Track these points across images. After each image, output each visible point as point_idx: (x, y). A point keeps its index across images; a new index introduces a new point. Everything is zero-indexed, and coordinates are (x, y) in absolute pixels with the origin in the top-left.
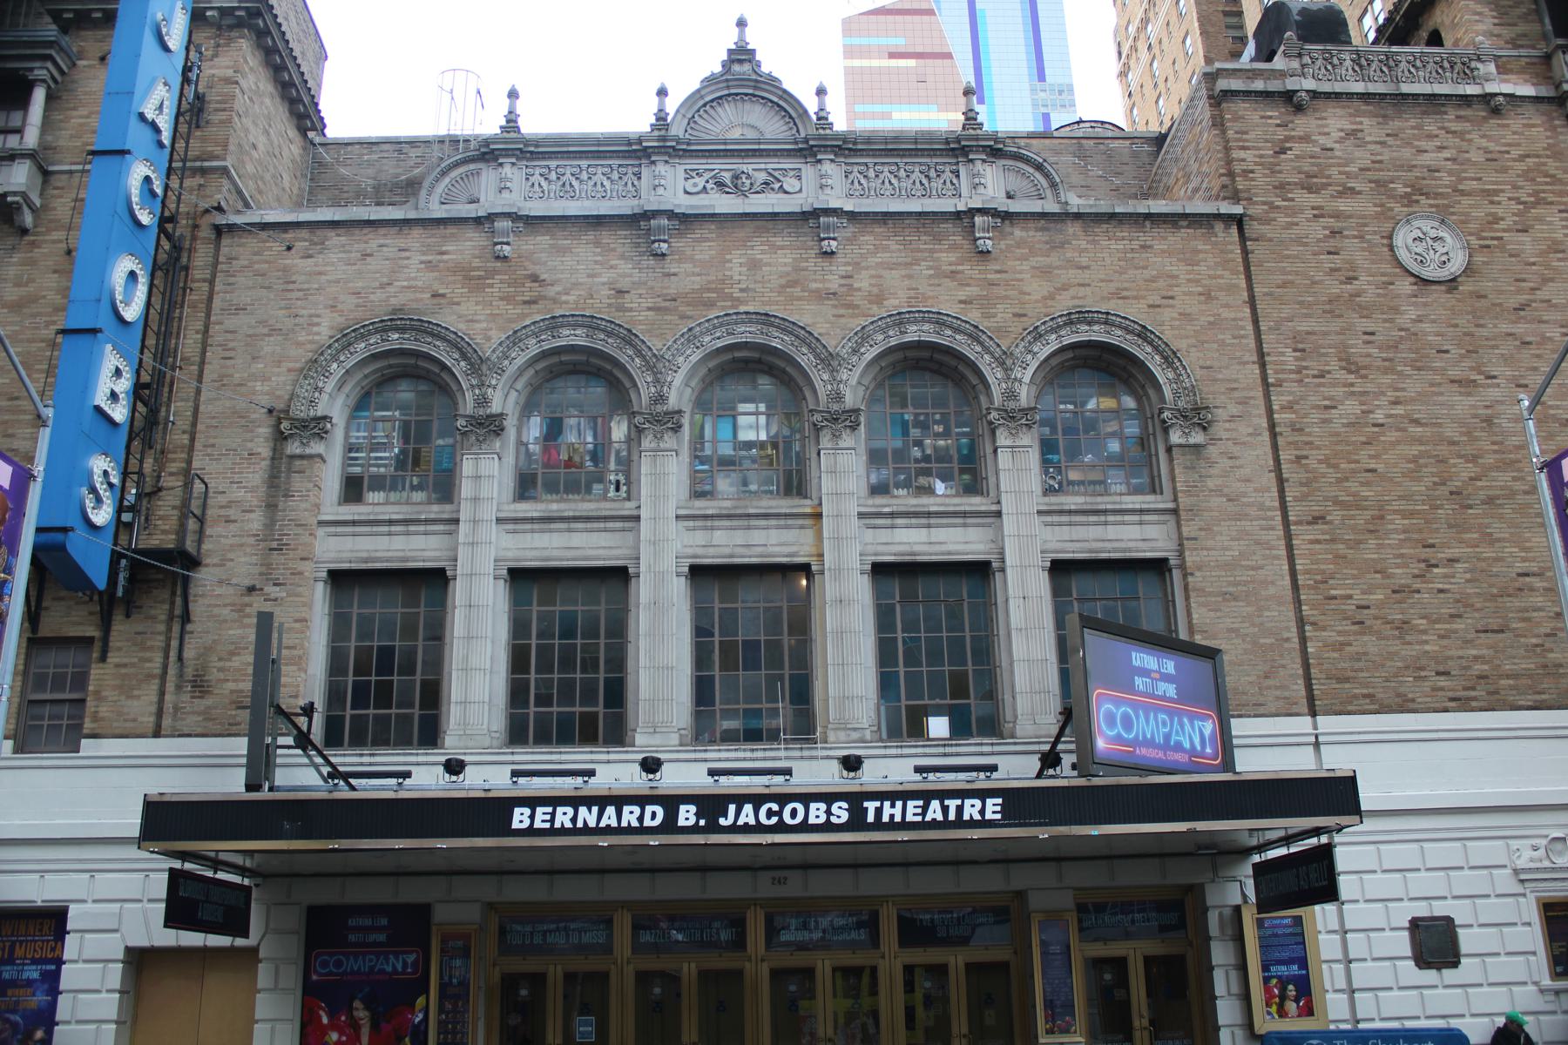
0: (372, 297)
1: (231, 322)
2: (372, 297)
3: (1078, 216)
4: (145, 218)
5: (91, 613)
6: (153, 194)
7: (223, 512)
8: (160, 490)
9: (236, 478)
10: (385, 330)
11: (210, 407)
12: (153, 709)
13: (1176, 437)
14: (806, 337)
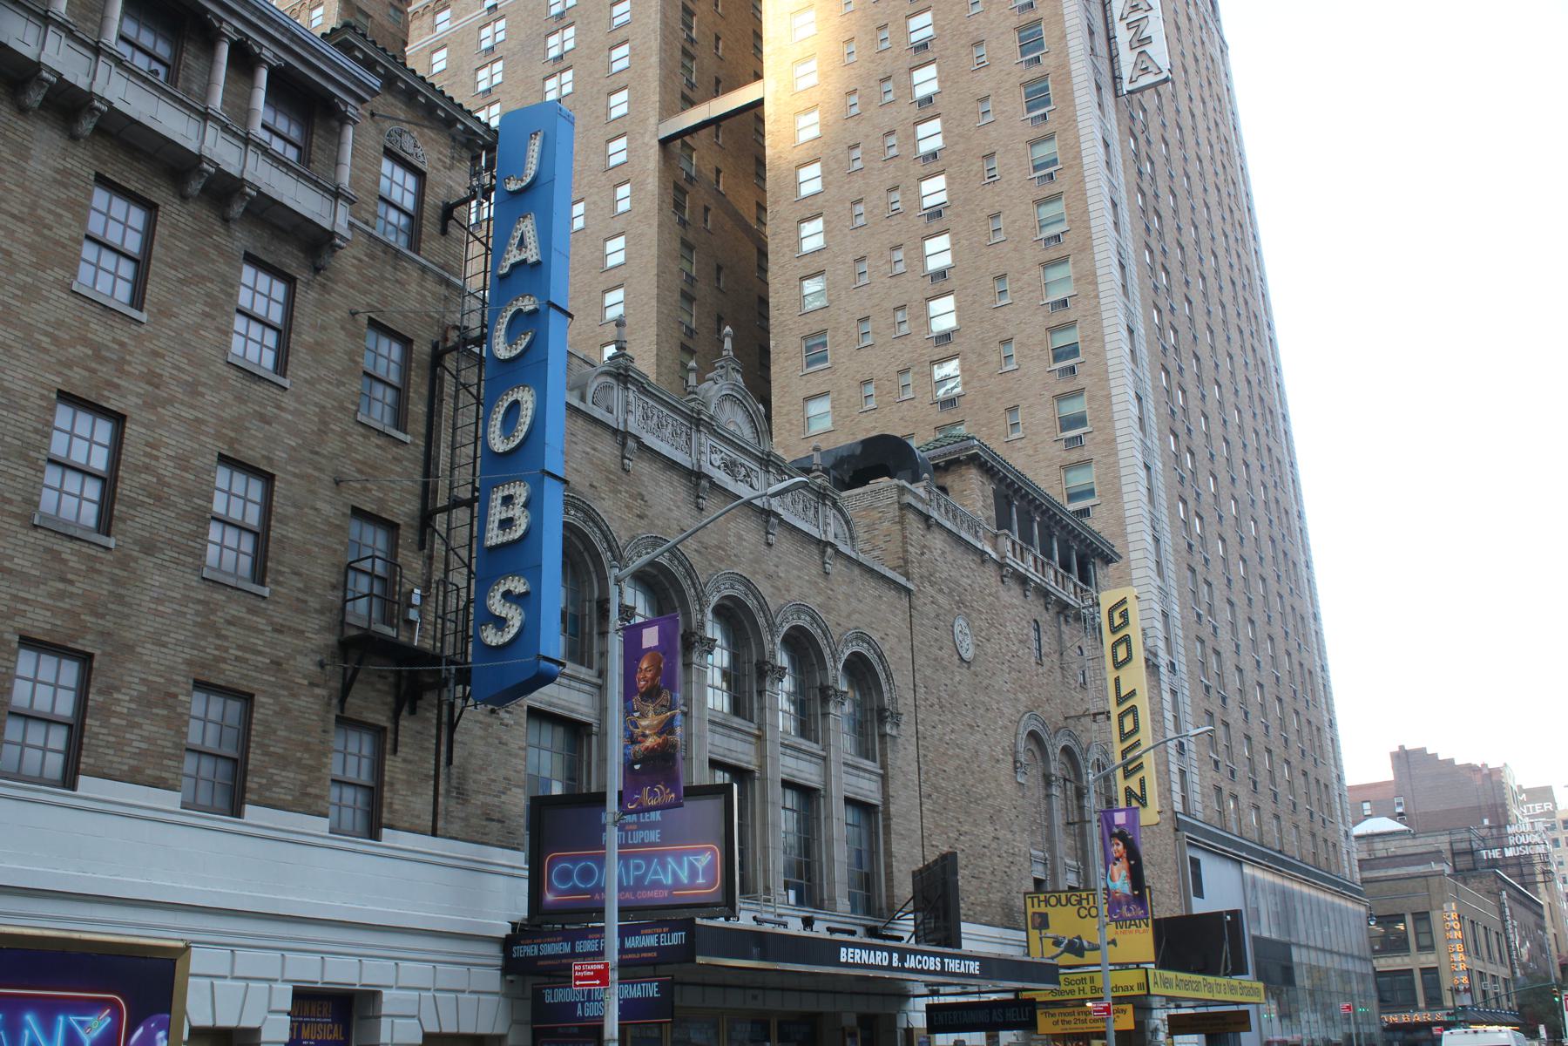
3: (860, 565)
5: (385, 704)
12: (431, 808)
13: (888, 729)
14: (763, 606)
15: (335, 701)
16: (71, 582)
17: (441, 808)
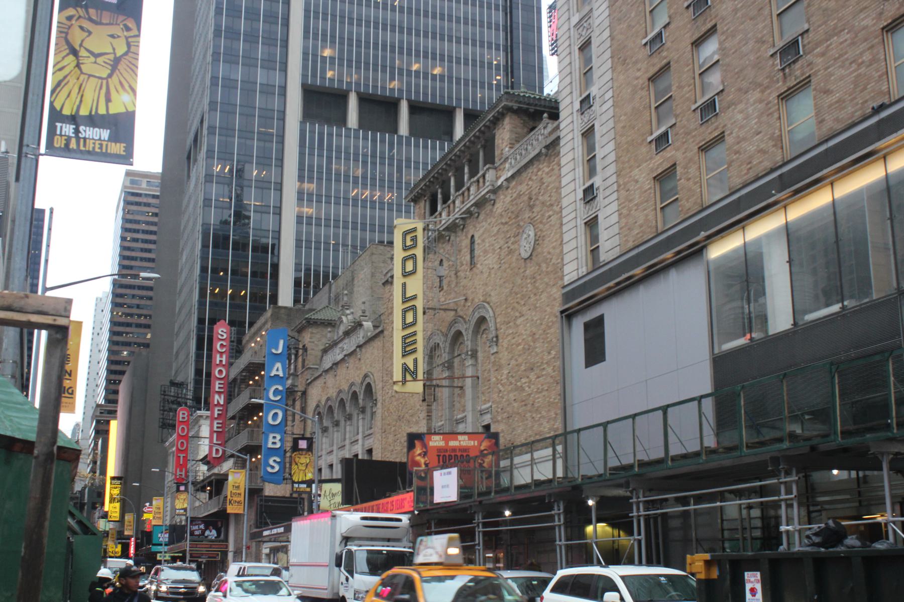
4: (278, 398)
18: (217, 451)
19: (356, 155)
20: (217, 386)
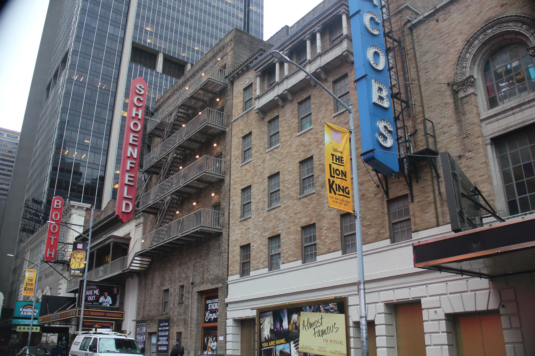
0: (475, 21)
1: (424, 59)
2: (475, 21)
4: (376, 33)
5: (405, 185)
6: (377, 24)
7: (441, 131)
8: (416, 131)
9: (443, 115)
10: (485, 31)
11: (426, 93)
12: (434, 216)
15: (385, 196)
16: (308, 207)
17: (440, 213)
18: (127, 205)
19: (161, 87)
20: (131, 138)
